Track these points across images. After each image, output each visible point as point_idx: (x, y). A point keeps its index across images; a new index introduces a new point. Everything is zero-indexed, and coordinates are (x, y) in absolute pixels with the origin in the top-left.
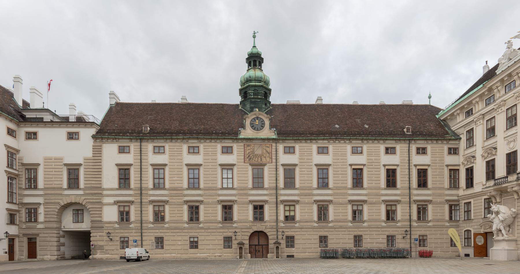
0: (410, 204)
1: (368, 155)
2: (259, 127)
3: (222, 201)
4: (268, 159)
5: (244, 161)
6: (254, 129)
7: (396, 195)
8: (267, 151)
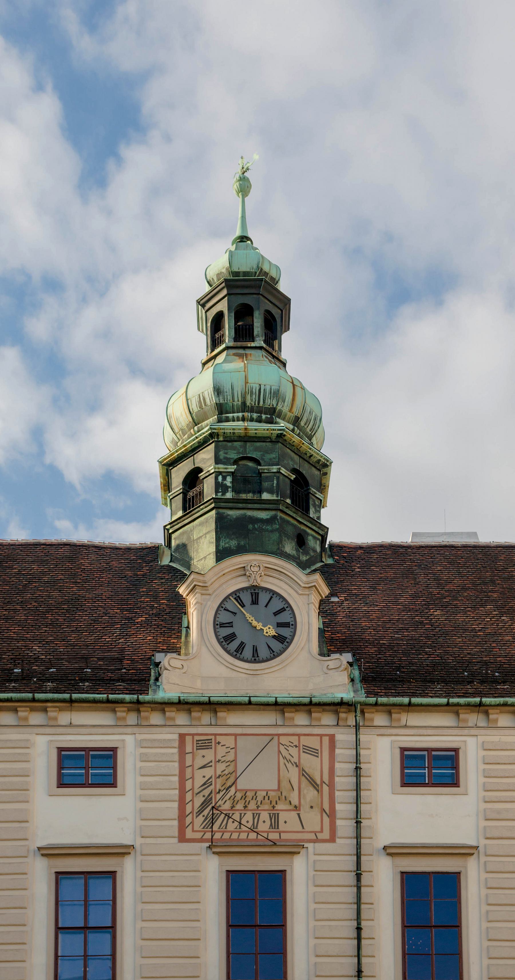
4: (313, 820)
8: (303, 773)
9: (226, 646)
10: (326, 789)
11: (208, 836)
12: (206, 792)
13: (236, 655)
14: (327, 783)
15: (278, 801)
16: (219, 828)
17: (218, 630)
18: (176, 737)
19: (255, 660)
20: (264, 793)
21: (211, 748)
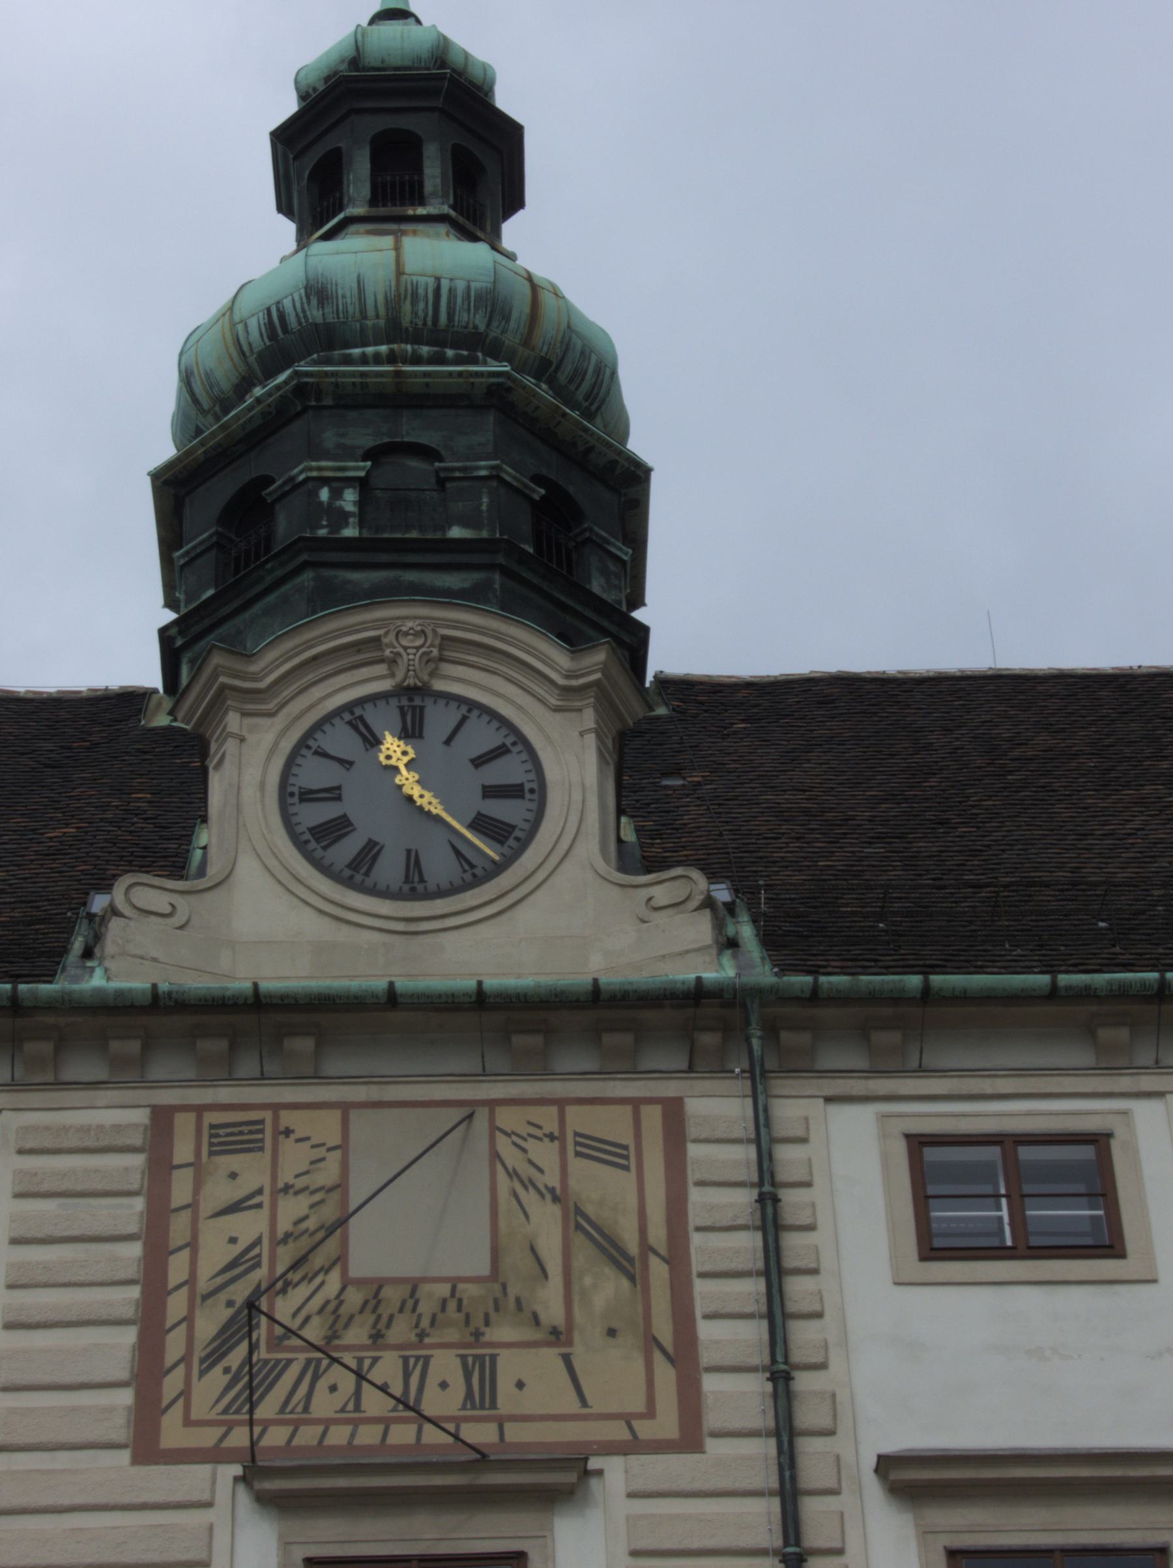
4: (618, 1376)
6: (358, 873)
8: (579, 1221)
9: (319, 853)
10: (659, 1270)
11: (239, 1438)
12: (241, 1292)
13: (351, 877)
14: (663, 1251)
15: (493, 1314)
16: (282, 1410)
17: (292, 810)
18: (140, 1117)
19: (413, 889)
20: (444, 1290)
21: (261, 1149)
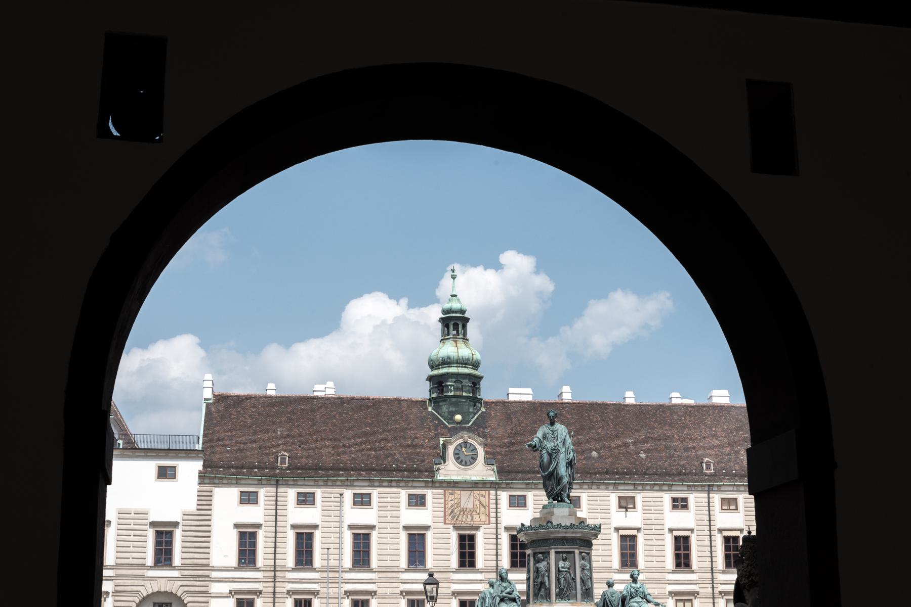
0: (713, 598)
1: (646, 511)
2: (469, 458)
3: (409, 593)
4: (483, 518)
5: (445, 520)
6: (461, 463)
7: (691, 583)
8: (481, 503)
